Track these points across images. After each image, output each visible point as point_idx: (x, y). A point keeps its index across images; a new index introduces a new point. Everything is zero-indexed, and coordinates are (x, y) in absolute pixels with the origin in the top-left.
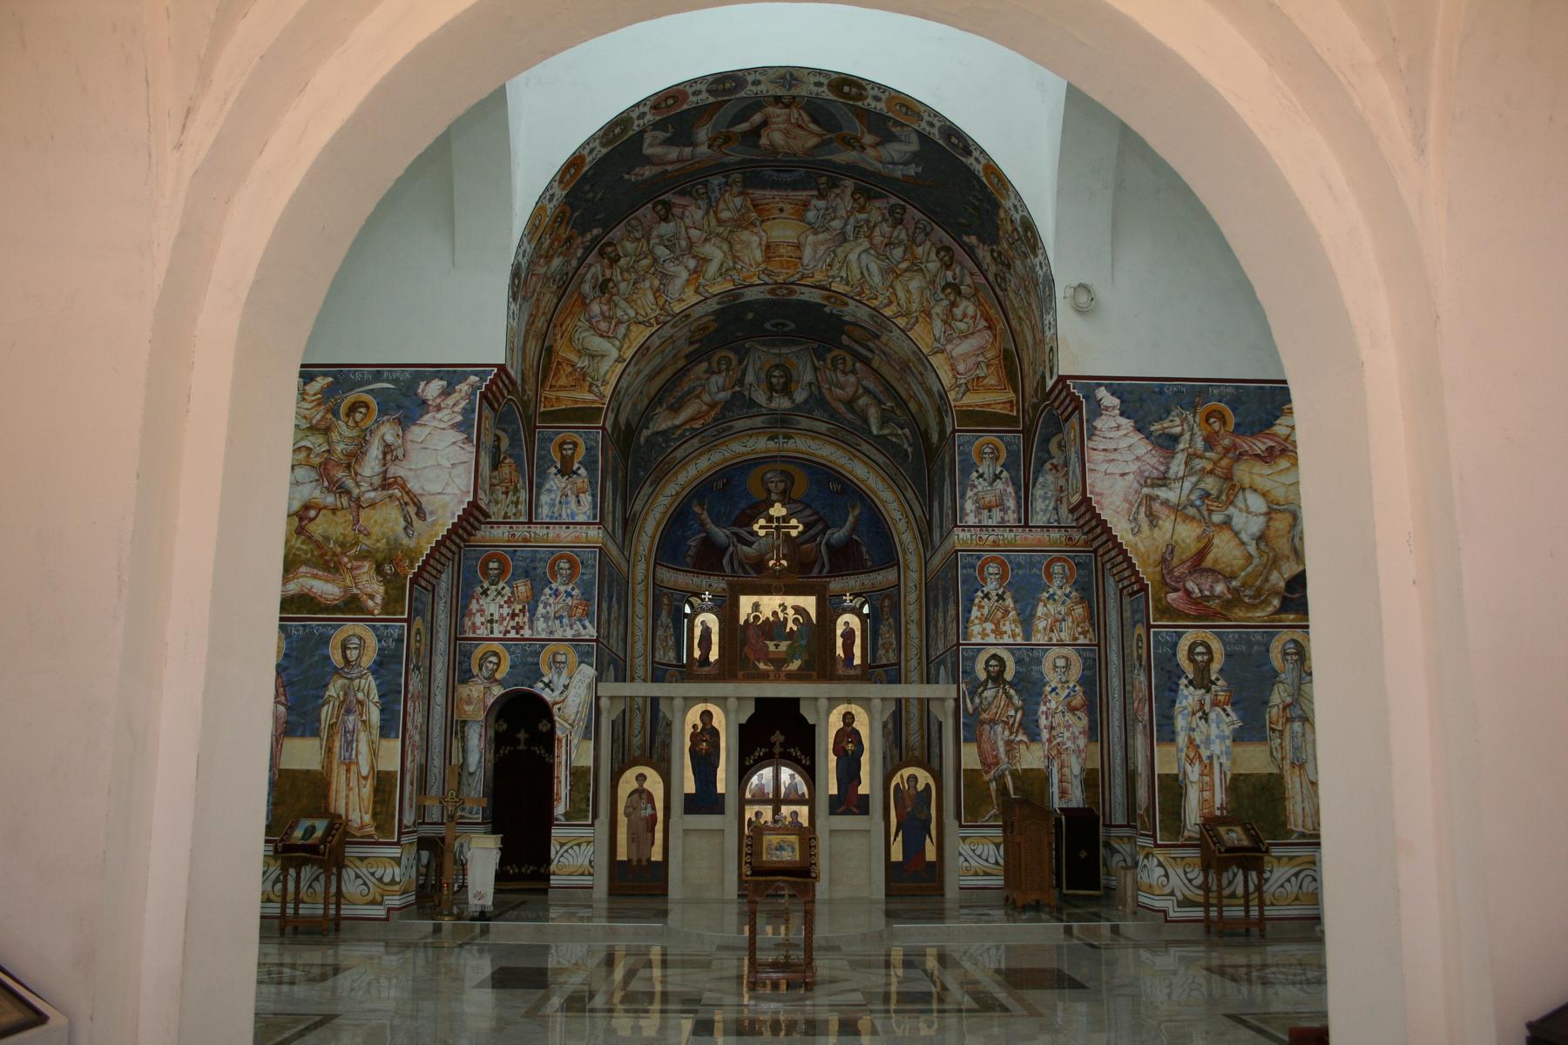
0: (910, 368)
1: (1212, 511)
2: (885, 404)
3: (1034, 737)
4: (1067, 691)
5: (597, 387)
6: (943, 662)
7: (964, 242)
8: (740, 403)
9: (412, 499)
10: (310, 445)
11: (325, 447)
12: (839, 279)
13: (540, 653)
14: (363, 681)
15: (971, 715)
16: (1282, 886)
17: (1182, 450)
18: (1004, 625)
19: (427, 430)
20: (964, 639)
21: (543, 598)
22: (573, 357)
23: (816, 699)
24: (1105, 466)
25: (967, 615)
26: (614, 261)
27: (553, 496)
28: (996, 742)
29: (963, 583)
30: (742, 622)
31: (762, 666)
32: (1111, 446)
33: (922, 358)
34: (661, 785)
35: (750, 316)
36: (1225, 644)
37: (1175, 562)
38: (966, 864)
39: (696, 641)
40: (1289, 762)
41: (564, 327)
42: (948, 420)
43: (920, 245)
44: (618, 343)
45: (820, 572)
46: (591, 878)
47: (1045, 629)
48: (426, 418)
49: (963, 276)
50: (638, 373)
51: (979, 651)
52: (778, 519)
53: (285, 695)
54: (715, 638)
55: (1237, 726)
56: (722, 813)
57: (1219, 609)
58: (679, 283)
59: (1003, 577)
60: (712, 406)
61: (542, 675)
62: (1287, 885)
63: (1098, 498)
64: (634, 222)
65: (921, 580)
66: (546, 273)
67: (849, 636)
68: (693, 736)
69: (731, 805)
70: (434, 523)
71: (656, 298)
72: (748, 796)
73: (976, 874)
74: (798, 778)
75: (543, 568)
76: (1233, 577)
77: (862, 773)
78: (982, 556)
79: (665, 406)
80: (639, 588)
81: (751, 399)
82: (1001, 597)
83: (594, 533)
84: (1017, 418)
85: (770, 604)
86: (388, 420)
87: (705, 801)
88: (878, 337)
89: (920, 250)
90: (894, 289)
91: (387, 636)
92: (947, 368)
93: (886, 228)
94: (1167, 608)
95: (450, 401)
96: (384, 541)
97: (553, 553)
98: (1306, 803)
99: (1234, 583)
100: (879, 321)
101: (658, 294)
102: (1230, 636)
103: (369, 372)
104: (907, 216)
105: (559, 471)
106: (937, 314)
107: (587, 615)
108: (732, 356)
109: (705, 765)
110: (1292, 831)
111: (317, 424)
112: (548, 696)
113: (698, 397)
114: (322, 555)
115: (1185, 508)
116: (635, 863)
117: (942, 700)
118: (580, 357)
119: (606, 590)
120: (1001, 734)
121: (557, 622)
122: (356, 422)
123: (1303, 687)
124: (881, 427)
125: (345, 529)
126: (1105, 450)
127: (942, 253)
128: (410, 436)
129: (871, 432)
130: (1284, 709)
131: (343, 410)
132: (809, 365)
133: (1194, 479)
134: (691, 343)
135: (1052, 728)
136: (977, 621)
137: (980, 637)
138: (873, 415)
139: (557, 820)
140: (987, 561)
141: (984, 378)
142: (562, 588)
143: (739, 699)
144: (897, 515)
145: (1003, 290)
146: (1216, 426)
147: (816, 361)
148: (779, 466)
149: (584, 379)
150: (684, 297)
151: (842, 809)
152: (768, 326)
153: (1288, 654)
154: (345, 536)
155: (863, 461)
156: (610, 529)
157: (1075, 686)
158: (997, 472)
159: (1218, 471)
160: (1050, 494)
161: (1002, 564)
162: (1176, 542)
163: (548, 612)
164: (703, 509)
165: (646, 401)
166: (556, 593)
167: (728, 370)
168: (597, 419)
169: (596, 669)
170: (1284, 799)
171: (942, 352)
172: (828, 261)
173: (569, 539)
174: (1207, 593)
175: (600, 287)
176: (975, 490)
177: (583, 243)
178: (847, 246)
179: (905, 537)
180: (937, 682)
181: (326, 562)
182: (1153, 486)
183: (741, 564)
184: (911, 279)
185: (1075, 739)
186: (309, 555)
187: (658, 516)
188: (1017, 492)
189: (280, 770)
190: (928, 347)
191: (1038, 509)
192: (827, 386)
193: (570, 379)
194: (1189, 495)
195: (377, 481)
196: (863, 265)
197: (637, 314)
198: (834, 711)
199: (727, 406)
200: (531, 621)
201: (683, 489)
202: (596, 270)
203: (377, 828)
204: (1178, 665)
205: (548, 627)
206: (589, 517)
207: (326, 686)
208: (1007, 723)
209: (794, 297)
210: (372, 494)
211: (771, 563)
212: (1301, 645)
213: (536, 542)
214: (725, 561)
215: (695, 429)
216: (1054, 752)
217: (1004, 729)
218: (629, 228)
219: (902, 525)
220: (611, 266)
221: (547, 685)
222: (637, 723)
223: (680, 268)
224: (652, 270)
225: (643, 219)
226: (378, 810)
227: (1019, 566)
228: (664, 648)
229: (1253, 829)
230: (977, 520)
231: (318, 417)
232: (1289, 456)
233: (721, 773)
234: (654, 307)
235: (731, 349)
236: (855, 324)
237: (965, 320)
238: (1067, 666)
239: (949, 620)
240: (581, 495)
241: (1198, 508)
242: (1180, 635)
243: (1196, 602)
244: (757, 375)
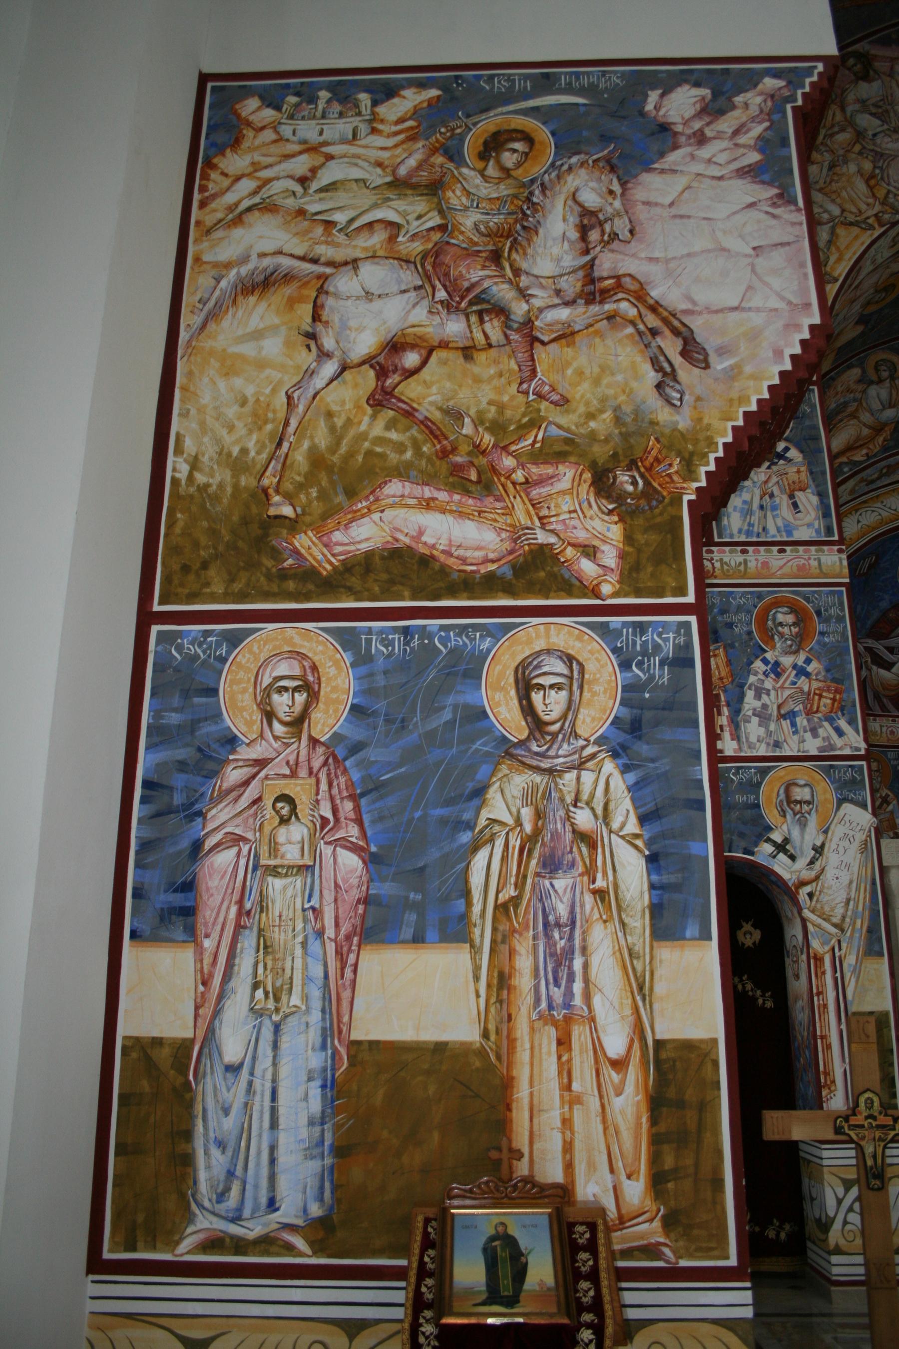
9: (665, 321)
10: (393, 216)
11: (435, 220)
13: (759, 784)
14: (587, 777)
19: (681, 182)
21: (752, 679)
48: (673, 158)
53: (359, 822)
60: (878, 429)
61: (769, 829)
70: (734, 373)
71: (871, 188)
86: (582, 164)
91: (644, 653)
95: (726, 124)
96: (608, 415)
97: (760, 596)
101: (872, 182)
103: (526, 77)
107: (842, 709)
111: (410, 175)
112: (782, 867)
113: (854, 416)
114: (444, 454)
121: (786, 724)
122: (506, 172)
125: (499, 391)
128: (639, 194)
131: (470, 146)
142: (787, 661)
154: (501, 408)
163: (765, 706)
166: (776, 670)
167: (892, 378)
169: (874, 814)
173: (786, 570)
181: (457, 470)
183: (877, 696)
186: (409, 455)
189: (355, 1045)
195: (571, 285)
197: (843, 211)
203: (670, 1222)
205: (769, 734)
206: (818, 532)
207: (480, 792)
210: (564, 314)
213: (728, 577)
215: (856, 463)
221: (781, 848)
224: (857, 148)
226: (669, 1162)
231: (412, 162)
234: (871, 201)
240: (799, 495)
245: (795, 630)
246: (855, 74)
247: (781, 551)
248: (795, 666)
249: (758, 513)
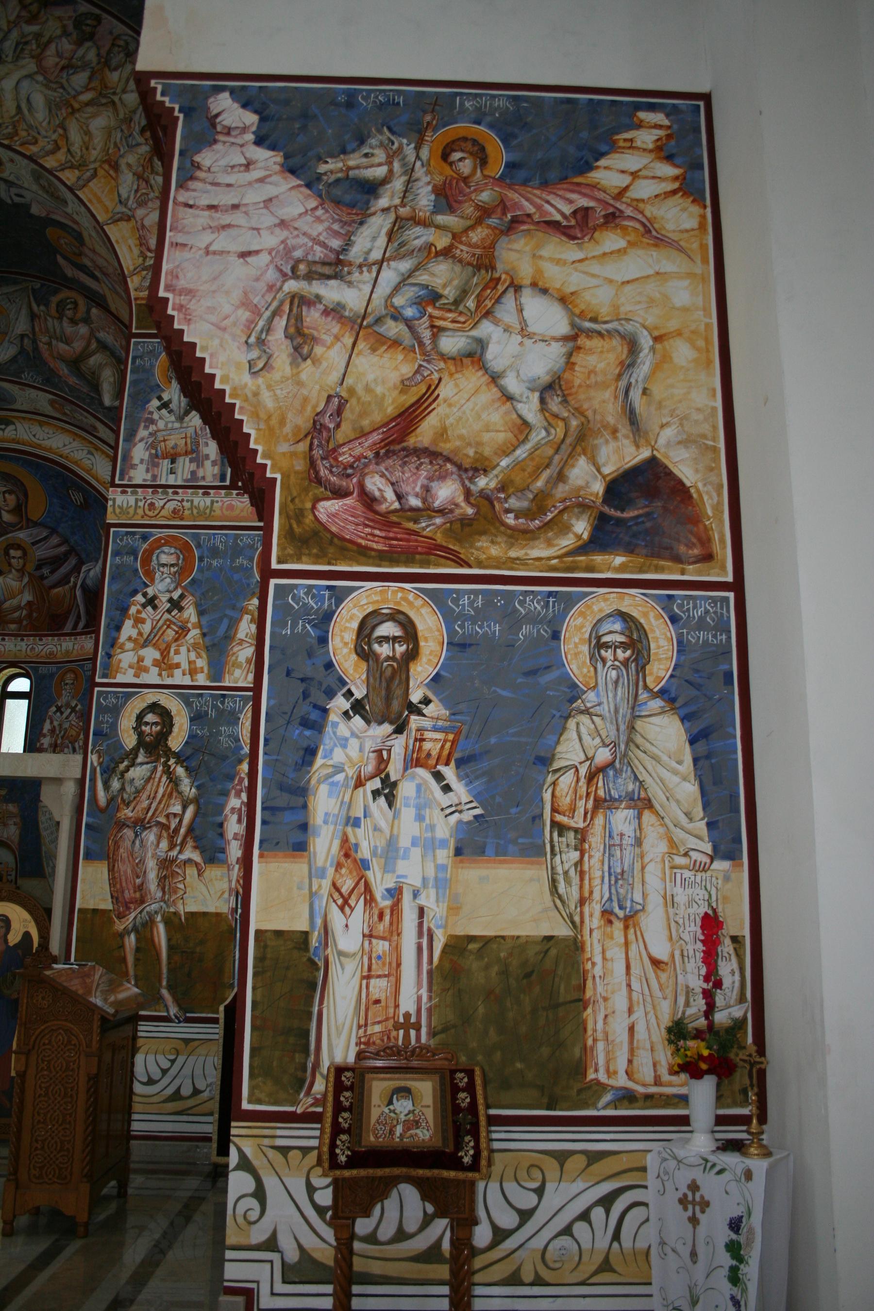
1: (442, 329)
15: (102, 811)
16: (567, 1231)
17: (385, 210)
18: (177, 652)
20: (105, 676)
24: (207, 238)
25: (114, 634)
28: (142, 861)
29: (113, 578)
32: (227, 198)
36: (449, 617)
37: (345, 431)
40: (597, 909)
43: (116, 69)
55: (468, 816)
57: (440, 538)
59: (182, 571)
62: (580, 1229)
63: (183, 300)
76: (481, 467)
78: (152, 535)
82: (176, 605)
89: (115, 76)
90: (65, 130)
92: (132, 242)
93: (66, 46)
94: (316, 533)
98: (639, 1014)
99: (482, 482)
102: (465, 600)
106: (129, 165)
110: (600, 1088)
115: (379, 320)
117: (58, 781)
123: (639, 724)
126: (211, 207)
129: (101, 403)
130: (591, 777)
132: (24, 312)
133: (405, 266)
136: (129, 645)
137: (131, 672)
146: (466, 167)
153: (606, 646)
159: (462, 251)
161: (185, 548)
162: (352, 391)
170: (581, 1002)
171: (129, 219)
174: (414, 502)
176: (152, 428)
182: (309, 277)
184: (94, 116)
190: (107, 211)
192: (45, 339)
194: (391, 296)
196: (23, 93)
204: (329, 665)
208: (165, 827)
212: (640, 627)
217: (159, 838)
227: (214, 552)
229: (470, 1088)
230: (149, 476)
232: (624, 229)
241: (409, 323)
242: (339, 596)
243: (386, 521)
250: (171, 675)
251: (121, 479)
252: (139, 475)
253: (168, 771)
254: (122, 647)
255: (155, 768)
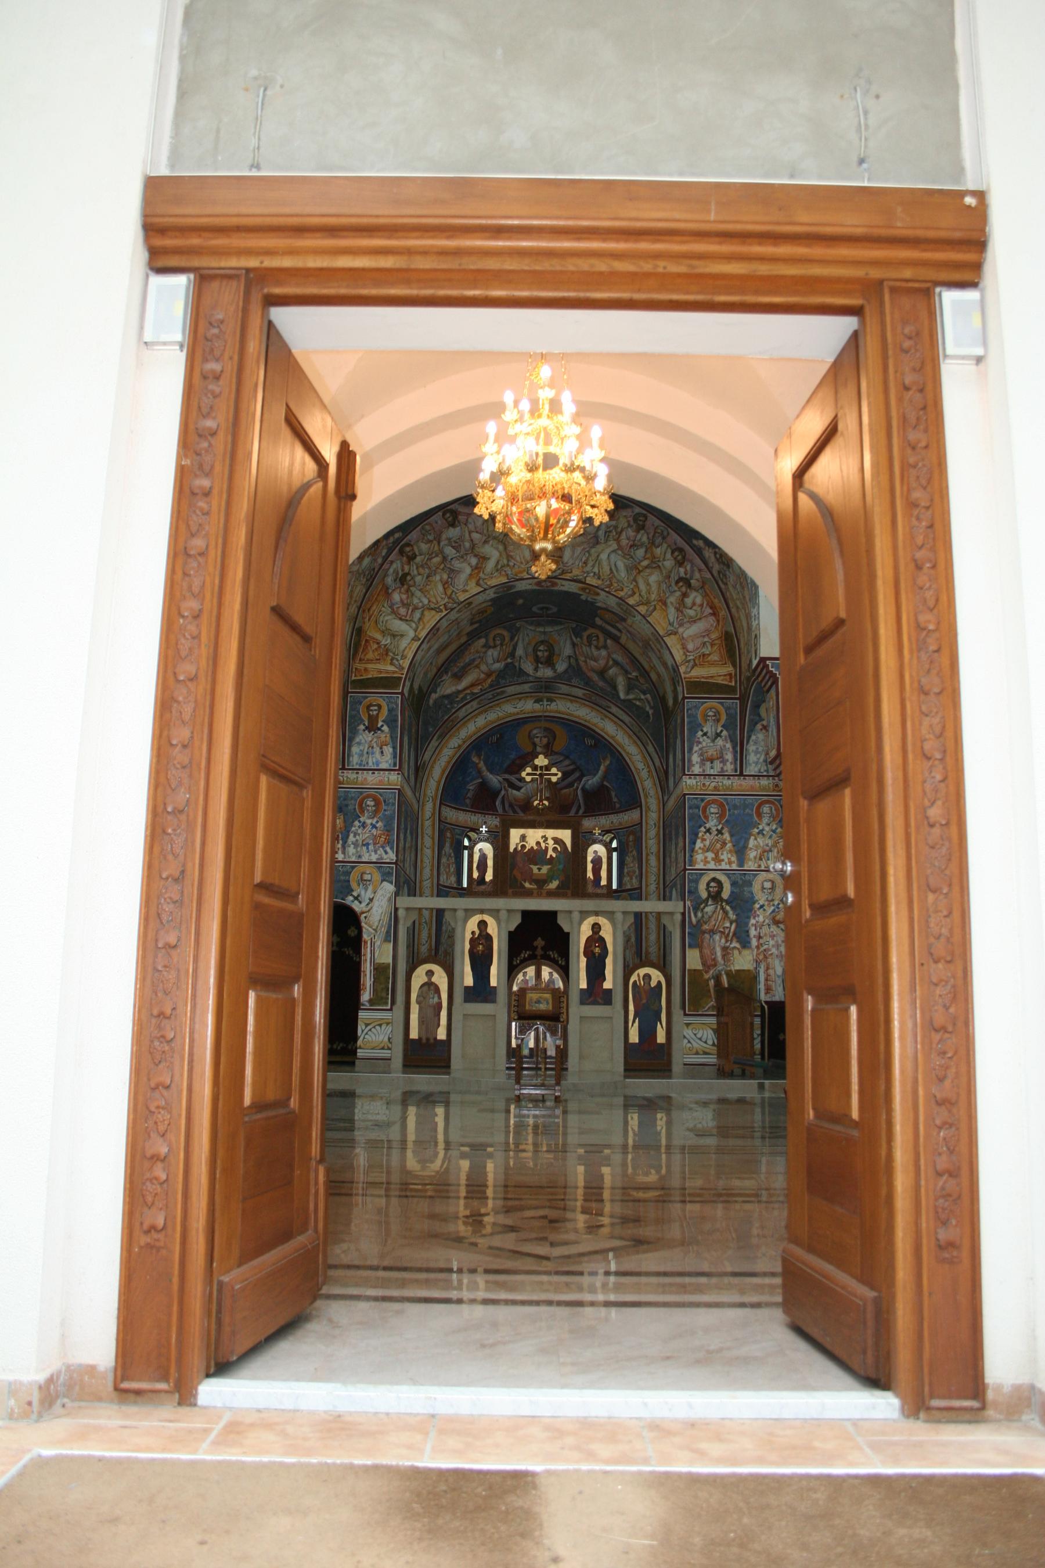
0: (650, 645)
2: (630, 674)
3: (745, 944)
4: (773, 908)
5: (398, 660)
6: (675, 885)
7: (695, 545)
8: (511, 673)
12: (592, 574)
15: (694, 926)
18: (722, 854)
21: (353, 829)
22: (378, 636)
23: (570, 912)
26: (412, 558)
27: (362, 748)
28: (714, 948)
29: (689, 820)
30: (512, 850)
31: (527, 885)
33: (659, 638)
34: (446, 979)
35: (521, 601)
38: (689, 1045)
39: (475, 865)
41: (371, 612)
42: (680, 689)
43: (658, 547)
44: (414, 625)
45: (577, 812)
46: (389, 1051)
47: (755, 858)
49: (693, 571)
50: (430, 648)
51: (702, 874)
52: (541, 768)
54: (490, 863)
56: (494, 1001)
58: (463, 577)
59: (721, 816)
60: (489, 675)
61: (352, 891)
64: (428, 527)
65: (659, 820)
66: (358, 570)
67: (597, 862)
68: (472, 941)
69: (502, 997)
71: (445, 589)
72: (515, 988)
73: (697, 1053)
74: (556, 975)
75: (353, 805)
77: (606, 972)
79: (449, 674)
80: (428, 823)
81: (520, 669)
82: (720, 832)
83: (394, 778)
84: (735, 687)
85: (534, 836)
87: (481, 992)
88: (624, 620)
89: (658, 551)
90: (636, 582)
92: (679, 646)
93: (631, 533)
97: (361, 793)
100: (625, 608)
101: (446, 586)
104: (648, 523)
105: (367, 728)
106: (672, 603)
107: (388, 843)
108: (506, 633)
109: (481, 963)
112: (356, 907)
113: (477, 667)
116: (424, 1041)
117: (672, 914)
118: (384, 636)
119: (403, 823)
120: (719, 941)
121: (365, 848)
124: (627, 693)
127: (676, 553)
129: (619, 697)
132: (568, 642)
134: (472, 624)
135: (760, 937)
136: (700, 851)
137: (702, 863)
138: (621, 683)
139: (363, 1005)
140: (709, 803)
141: (709, 655)
142: (369, 822)
143: (509, 911)
144: (640, 766)
145: (726, 584)
147: (574, 639)
148: (544, 724)
149: (387, 654)
150: (468, 588)
151: (590, 1000)
152: (535, 609)
155: (612, 720)
156: (406, 775)
157: (779, 904)
158: (718, 731)
160: (760, 749)
161: (721, 805)
163: (357, 840)
164: (480, 759)
165: (435, 670)
166: (364, 825)
167: (502, 645)
168: (397, 686)
169: (395, 886)
171: (675, 633)
172: (584, 559)
173: (374, 782)
175: (400, 580)
176: (700, 746)
177: (386, 545)
178: (599, 548)
179: (647, 783)
180: (670, 899)
183: (511, 806)
184: (650, 575)
185: (778, 946)
187: (443, 764)
188: (734, 747)
191: (751, 762)
192: (583, 659)
193: (376, 653)
197: (429, 601)
198: (585, 922)
199: (501, 674)
200: (344, 847)
201: (464, 742)
202: (397, 565)
205: (357, 852)
206: (390, 765)
208: (723, 933)
209: (556, 588)
211: (536, 803)
213: (348, 784)
214: (498, 803)
215: (473, 694)
216: (761, 957)
218: (423, 532)
219: (644, 774)
220: (409, 563)
221: (356, 898)
222: (424, 934)
223: (465, 565)
224: (442, 566)
225: (434, 525)
227: (735, 807)
228: (447, 873)
230: (701, 770)
233: (494, 970)
234: (443, 596)
235: (505, 628)
236: (606, 610)
237: (694, 608)
238: (773, 888)
239: (679, 850)
240: (384, 747)
244: (525, 649)
245: (374, 808)
246: (448, 523)
247: (373, 773)
248: (372, 824)
249: (365, 755)
250: (720, 865)
251: (688, 771)
252: (697, 770)
253: (722, 908)
254: (697, 852)
255: (717, 908)
